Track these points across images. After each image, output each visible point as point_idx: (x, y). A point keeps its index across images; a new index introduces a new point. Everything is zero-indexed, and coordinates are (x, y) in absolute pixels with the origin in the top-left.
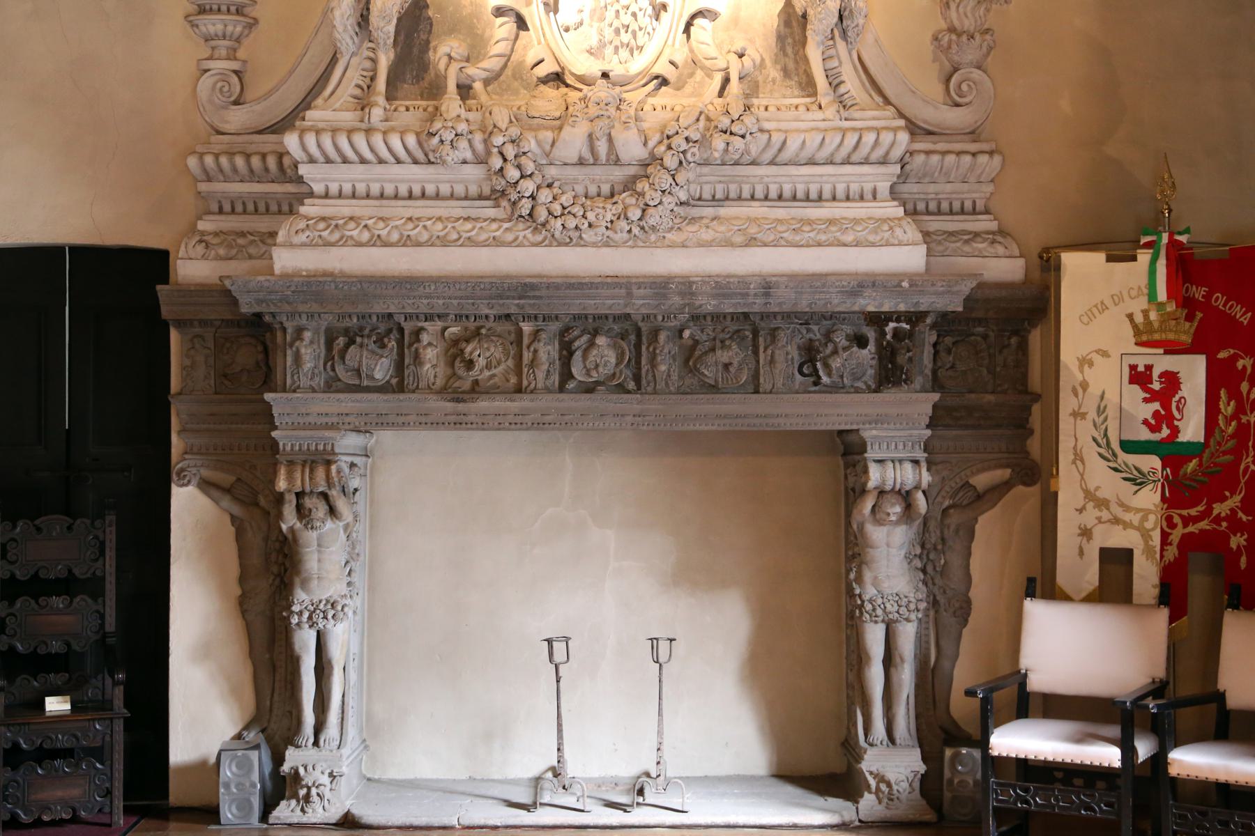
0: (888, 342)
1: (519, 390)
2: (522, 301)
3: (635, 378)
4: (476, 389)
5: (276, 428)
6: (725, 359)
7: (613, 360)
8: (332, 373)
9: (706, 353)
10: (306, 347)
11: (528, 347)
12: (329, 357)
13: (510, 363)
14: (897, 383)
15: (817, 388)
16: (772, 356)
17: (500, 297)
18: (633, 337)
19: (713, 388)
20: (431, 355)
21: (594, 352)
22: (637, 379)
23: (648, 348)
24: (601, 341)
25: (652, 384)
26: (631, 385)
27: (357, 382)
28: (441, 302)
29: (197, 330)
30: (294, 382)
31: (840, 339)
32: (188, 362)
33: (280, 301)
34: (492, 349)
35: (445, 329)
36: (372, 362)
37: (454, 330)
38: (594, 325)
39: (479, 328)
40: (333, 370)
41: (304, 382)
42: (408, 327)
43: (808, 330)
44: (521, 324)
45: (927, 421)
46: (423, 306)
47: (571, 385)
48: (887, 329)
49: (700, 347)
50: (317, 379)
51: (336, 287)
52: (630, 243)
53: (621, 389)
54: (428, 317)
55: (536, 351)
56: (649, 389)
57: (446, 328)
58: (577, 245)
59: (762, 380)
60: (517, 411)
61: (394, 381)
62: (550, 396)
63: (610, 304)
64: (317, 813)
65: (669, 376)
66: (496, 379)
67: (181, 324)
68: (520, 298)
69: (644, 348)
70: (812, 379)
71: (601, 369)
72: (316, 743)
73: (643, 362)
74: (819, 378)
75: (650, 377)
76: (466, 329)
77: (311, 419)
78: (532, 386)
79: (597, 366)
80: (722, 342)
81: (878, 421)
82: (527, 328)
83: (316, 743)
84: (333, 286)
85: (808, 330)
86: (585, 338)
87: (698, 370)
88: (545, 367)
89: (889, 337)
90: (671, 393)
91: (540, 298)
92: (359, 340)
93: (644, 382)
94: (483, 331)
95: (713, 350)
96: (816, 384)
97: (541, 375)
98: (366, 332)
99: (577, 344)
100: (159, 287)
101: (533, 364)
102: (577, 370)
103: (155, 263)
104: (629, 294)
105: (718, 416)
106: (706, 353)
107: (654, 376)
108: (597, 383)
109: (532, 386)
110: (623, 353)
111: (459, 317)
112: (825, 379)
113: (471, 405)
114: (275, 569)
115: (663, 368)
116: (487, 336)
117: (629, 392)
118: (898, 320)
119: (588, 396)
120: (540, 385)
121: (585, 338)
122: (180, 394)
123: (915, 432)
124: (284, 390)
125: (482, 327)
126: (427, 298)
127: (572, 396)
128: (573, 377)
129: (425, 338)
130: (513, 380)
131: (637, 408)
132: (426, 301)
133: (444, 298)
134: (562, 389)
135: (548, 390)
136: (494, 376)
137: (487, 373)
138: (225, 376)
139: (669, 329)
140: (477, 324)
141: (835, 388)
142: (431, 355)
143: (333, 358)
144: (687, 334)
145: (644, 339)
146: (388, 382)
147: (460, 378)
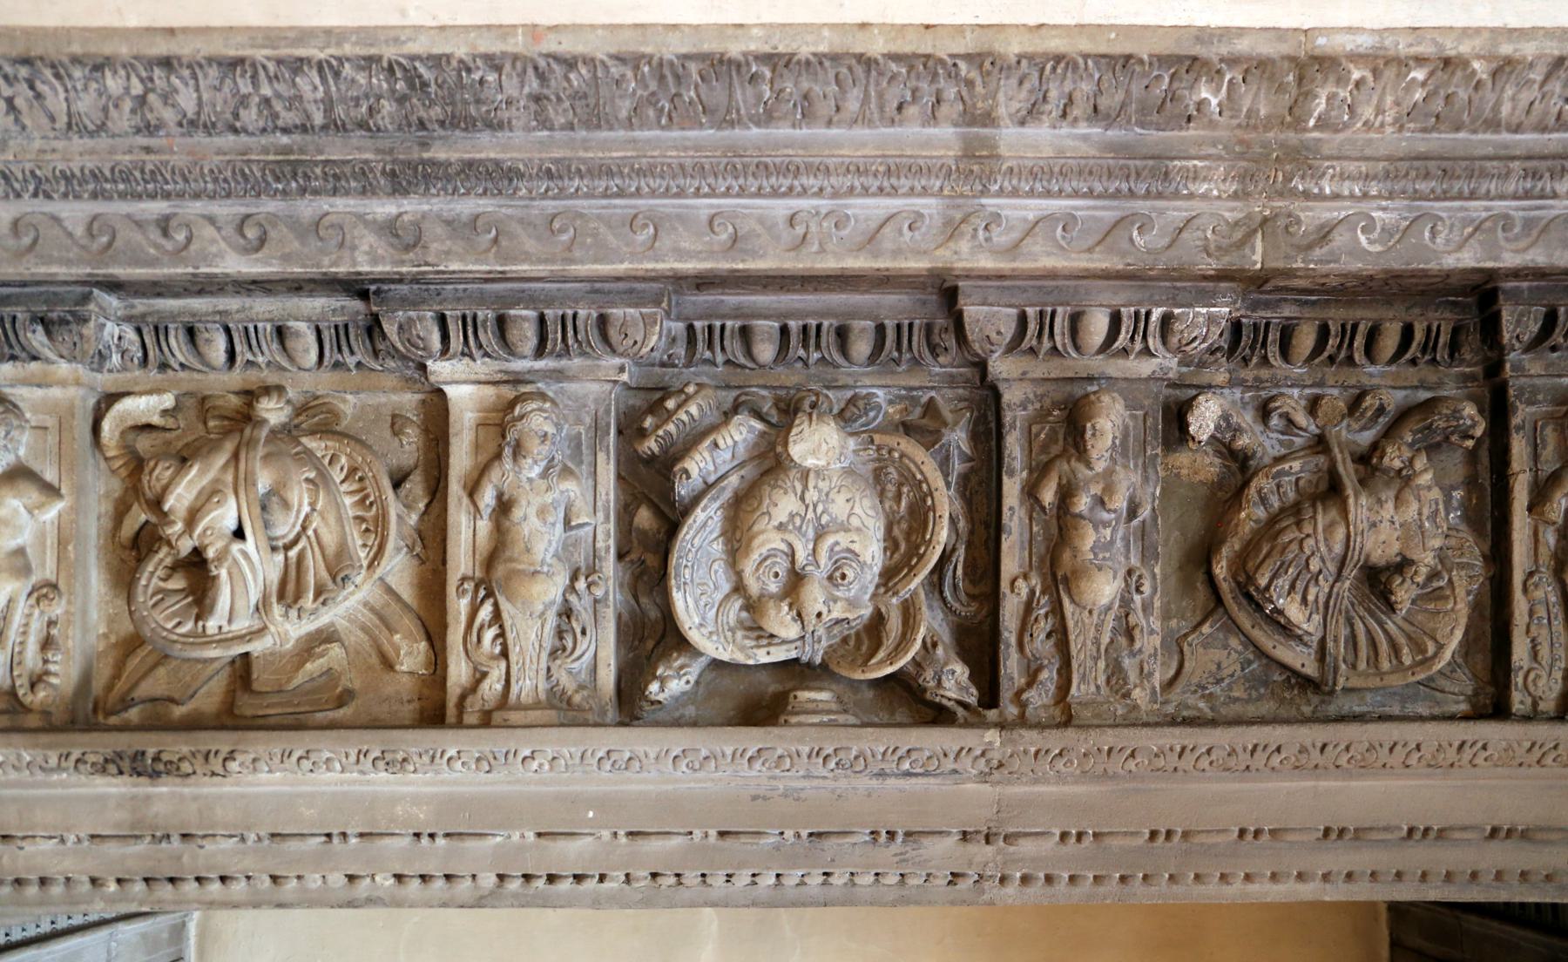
1: (434, 710)
3: (963, 649)
4: (249, 705)
6: (1381, 545)
7: (873, 552)
9: (1295, 511)
11: (472, 490)
13: (398, 568)
18: (958, 437)
21: (784, 505)
22: (979, 644)
23: (1031, 492)
24: (817, 444)
25: (1049, 676)
34: (299, 496)
44: (440, 369)
47: (672, 684)
49: (1261, 483)
53: (909, 700)
55: (504, 506)
56: (1040, 699)
57: (111, 398)
60: (422, 817)
62: (567, 744)
69: (1012, 489)
71: (815, 597)
73: (1011, 564)
75: (1040, 644)
78: (492, 686)
79: (796, 580)
80: (1367, 460)
82: (466, 387)
87: (1254, 600)
88: (550, 590)
90: (1132, 721)
93: (1011, 666)
95: (1331, 491)
97: (530, 631)
99: (699, 465)
101: (496, 571)
102: (699, 602)
106: (1295, 511)
107: (1060, 635)
108: (796, 671)
109: (492, 686)
110: (920, 515)
113: (208, 788)
115: (1104, 589)
116: (288, 432)
117: (939, 715)
119: (752, 738)
120: (528, 685)
121: (741, 433)
127: (678, 740)
128: (682, 644)
130: (411, 655)
131: (976, 796)
134: (630, 703)
135: (564, 710)
136: (326, 636)
137: (289, 629)
139: (1128, 387)
144: (1205, 418)
145: (1014, 445)
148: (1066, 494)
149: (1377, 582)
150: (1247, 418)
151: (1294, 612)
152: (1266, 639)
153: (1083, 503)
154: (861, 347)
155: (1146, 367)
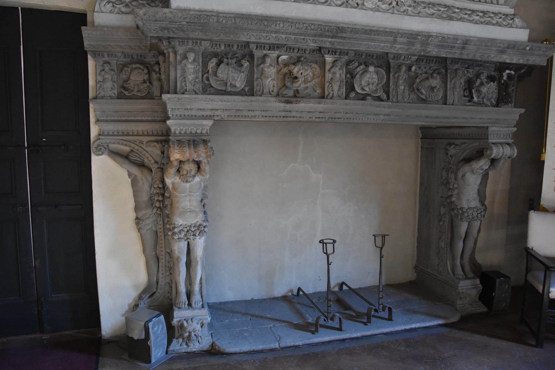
0: (505, 81)
1: (323, 97)
2: (333, 40)
3: (387, 93)
4: (297, 95)
5: (169, 118)
6: (434, 85)
8: (206, 82)
10: (191, 63)
12: (205, 71)
14: (506, 103)
15: (469, 104)
16: (454, 85)
17: (321, 36)
19: (424, 101)
20: (271, 71)
22: (388, 93)
23: (394, 76)
24: (371, 69)
26: (385, 97)
27: (223, 88)
28: (284, 36)
29: (106, 58)
30: (182, 88)
31: (483, 78)
32: (100, 78)
33: (177, 29)
35: (278, 57)
36: (236, 75)
37: (284, 57)
38: (366, 59)
39: (299, 58)
40: (208, 79)
41: (189, 87)
42: (258, 54)
43: (468, 72)
44: (326, 56)
45: (515, 123)
46: (272, 39)
47: (353, 95)
48: (504, 74)
50: (197, 86)
51: (218, 21)
52: (390, 11)
53: (379, 99)
54: (272, 47)
56: (394, 100)
58: (362, 9)
59: (448, 98)
60: (321, 110)
61: (247, 89)
63: (379, 46)
64: (195, 347)
65: (404, 92)
66: (308, 90)
67: (96, 54)
68: (332, 38)
70: (468, 99)
72: (190, 305)
73: (391, 84)
74: (472, 98)
75: (394, 93)
76: (291, 58)
77: (193, 113)
80: (432, 75)
81: (496, 122)
82: (329, 59)
83: (190, 305)
84: (215, 20)
85: (468, 72)
86: (362, 67)
89: (505, 78)
90: (405, 102)
91: (344, 38)
92: (225, 60)
94: (302, 59)
96: (469, 101)
97: (336, 88)
98: (230, 56)
100: (83, 28)
103: (79, 19)
104: (395, 41)
105: (427, 117)
107: (397, 92)
111: (290, 49)
112: (475, 99)
113: (297, 105)
114: (157, 205)
117: (382, 100)
118: (511, 70)
120: (336, 94)
122: (96, 98)
123: (511, 129)
124: (176, 93)
125: (302, 57)
126: (276, 32)
129: (268, 60)
131: (387, 111)
132: (274, 35)
133: (286, 34)
136: (307, 88)
138: (124, 88)
140: (298, 55)
141: (479, 104)
142: (271, 71)
143: (208, 72)
144: (413, 68)
146: (243, 89)
147: (287, 87)
148: (398, 77)
149: (432, 89)
150: (417, 69)
151: (424, 92)
152: (419, 94)
153: (400, 78)
154: (375, 57)
155: (407, 62)
